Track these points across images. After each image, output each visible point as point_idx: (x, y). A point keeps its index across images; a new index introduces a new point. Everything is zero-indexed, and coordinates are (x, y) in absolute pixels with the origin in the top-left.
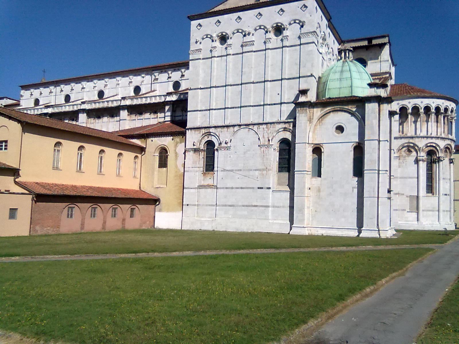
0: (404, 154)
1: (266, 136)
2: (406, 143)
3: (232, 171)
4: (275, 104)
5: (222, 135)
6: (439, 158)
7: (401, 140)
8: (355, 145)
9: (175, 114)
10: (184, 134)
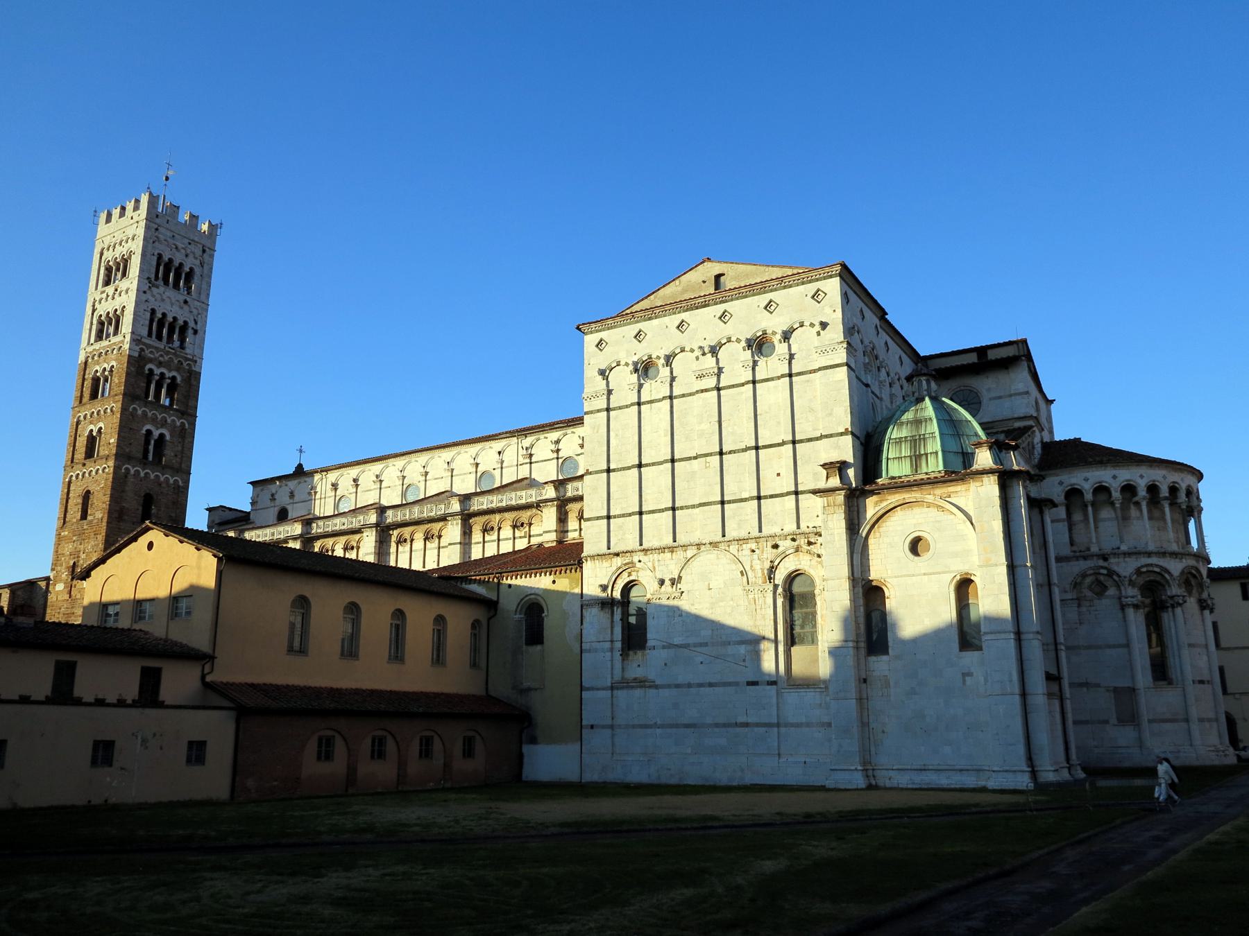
0: (1089, 594)
3: (686, 646)
5: (661, 568)
6: (1172, 597)
8: (958, 578)
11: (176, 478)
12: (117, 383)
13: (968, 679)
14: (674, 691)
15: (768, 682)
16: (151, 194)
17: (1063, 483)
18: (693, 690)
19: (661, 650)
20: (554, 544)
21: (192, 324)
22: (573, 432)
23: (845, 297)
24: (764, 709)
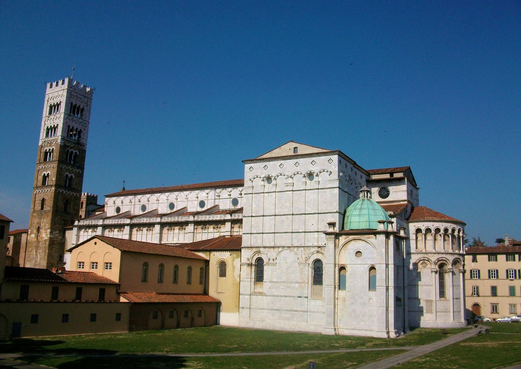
1: (304, 257)
2: (421, 258)
3: (277, 282)
4: (310, 232)
5: (269, 254)
7: (418, 255)
8: (370, 266)
10: (241, 250)
12: (55, 155)
13: (371, 300)
16: (69, 79)
17: (415, 226)
18: (279, 298)
19: (269, 283)
20: (230, 236)
21: (83, 130)
23: (340, 162)
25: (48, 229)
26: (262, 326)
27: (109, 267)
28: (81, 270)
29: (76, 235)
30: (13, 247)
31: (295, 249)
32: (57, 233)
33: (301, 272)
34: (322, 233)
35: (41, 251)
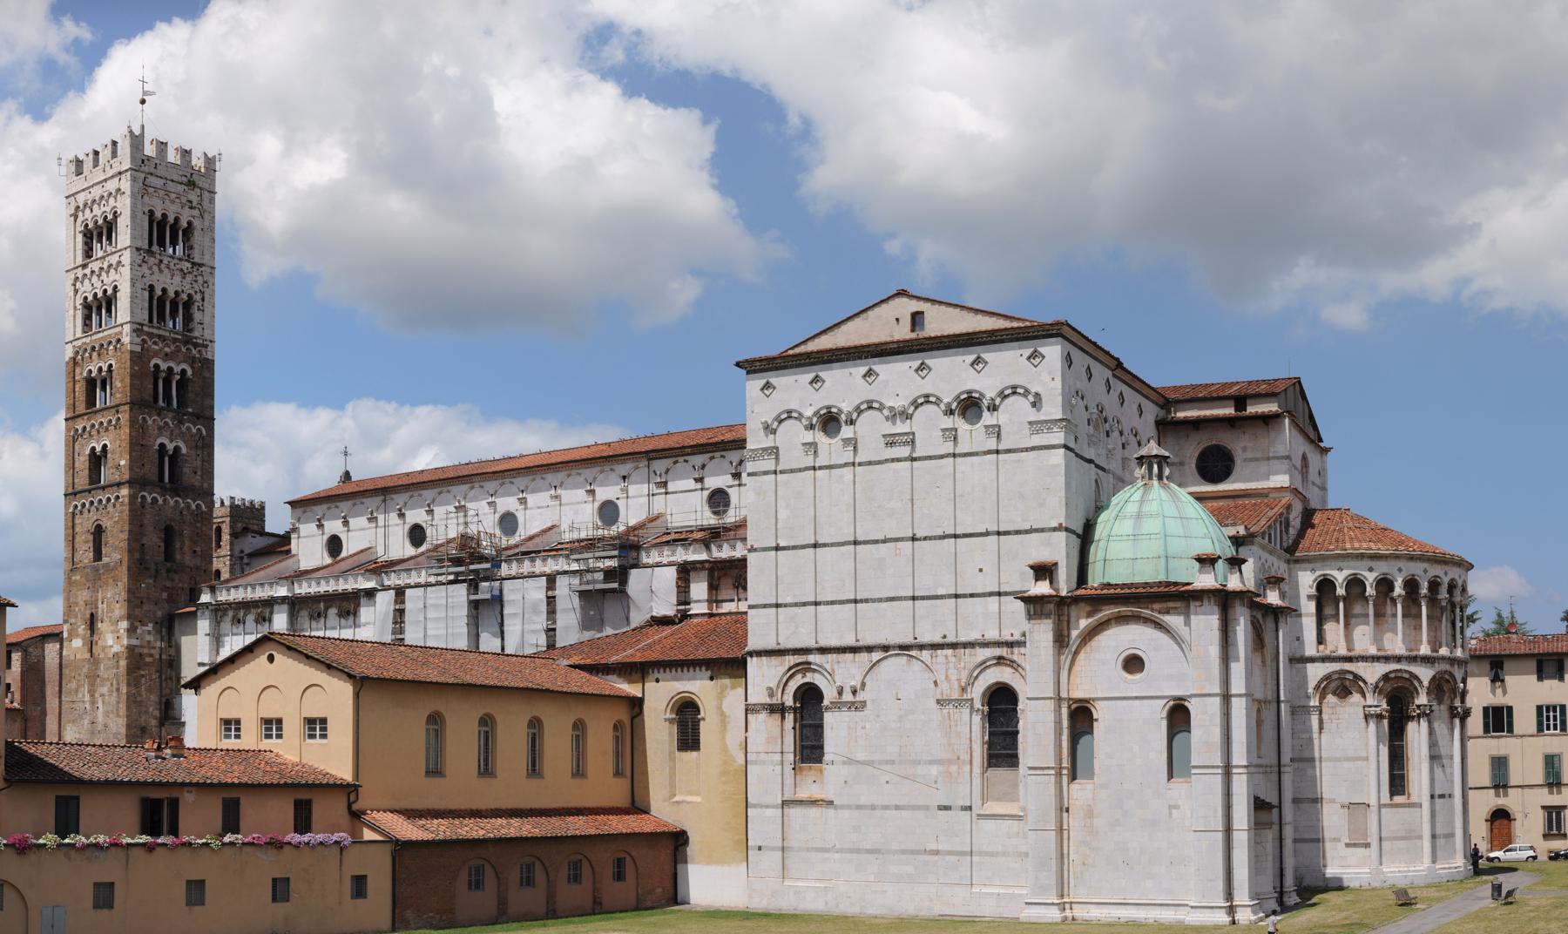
1: (953, 678)
4: (972, 595)
8: (1172, 703)
9: (716, 595)
11: (198, 502)
13: (1174, 811)
14: (856, 813)
15: (962, 807)
18: (878, 813)
19: (841, 767)
22: (723, 457)
24: (957, 836)
25: (121, 619)
26: (826, 903)
27: (318, 733)
28: (232, 743)
29: (206, 635)
30: (22, 680)
31: (926, 655)
32: (149, 632)
33: (948, 730)
34: (1011, 598)
35: (105, 690)
